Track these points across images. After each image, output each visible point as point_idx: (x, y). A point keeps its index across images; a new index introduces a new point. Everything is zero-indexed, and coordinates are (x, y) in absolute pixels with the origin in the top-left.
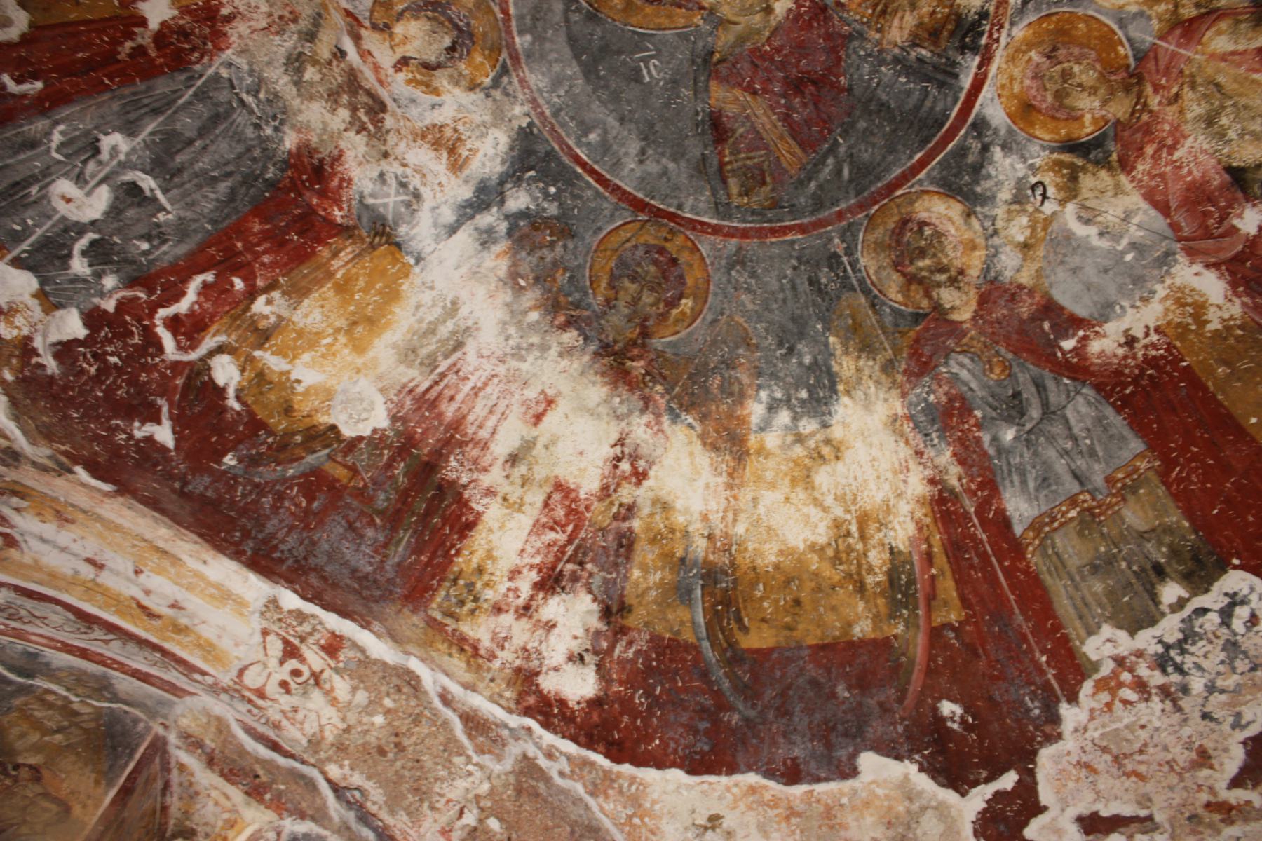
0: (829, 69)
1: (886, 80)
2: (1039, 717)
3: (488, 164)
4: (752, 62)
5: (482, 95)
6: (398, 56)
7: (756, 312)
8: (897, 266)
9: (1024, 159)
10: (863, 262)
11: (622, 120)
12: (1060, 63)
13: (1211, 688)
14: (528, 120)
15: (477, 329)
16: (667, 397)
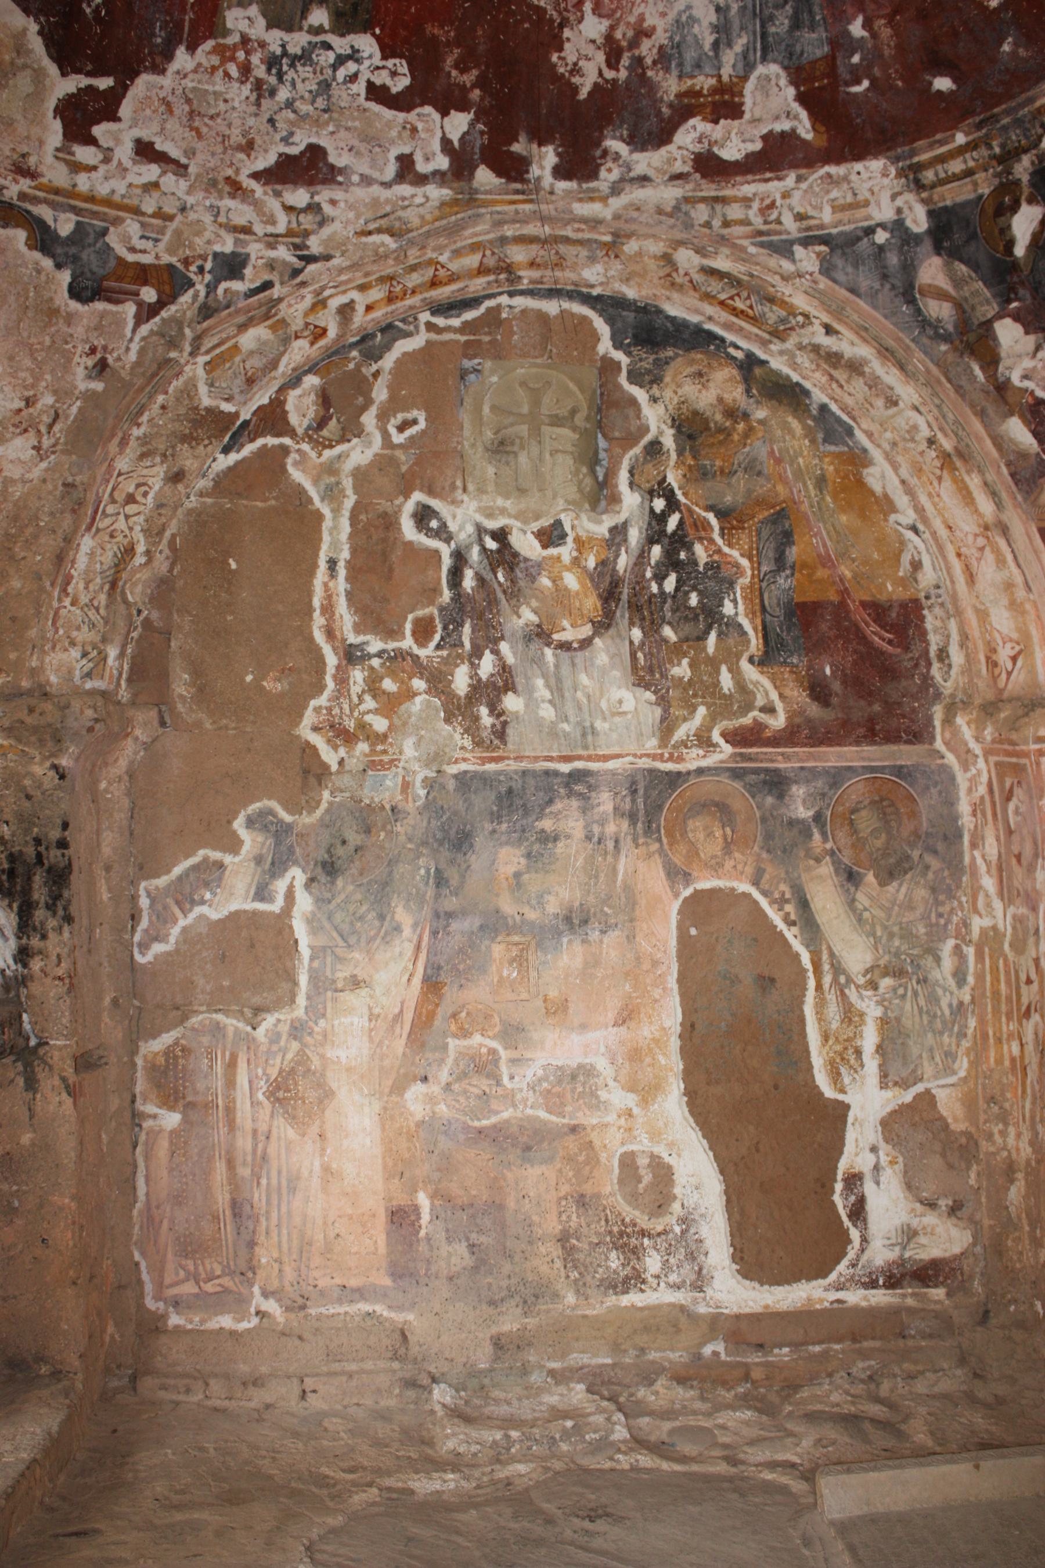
2: (158, 45)
13: (289, 104)
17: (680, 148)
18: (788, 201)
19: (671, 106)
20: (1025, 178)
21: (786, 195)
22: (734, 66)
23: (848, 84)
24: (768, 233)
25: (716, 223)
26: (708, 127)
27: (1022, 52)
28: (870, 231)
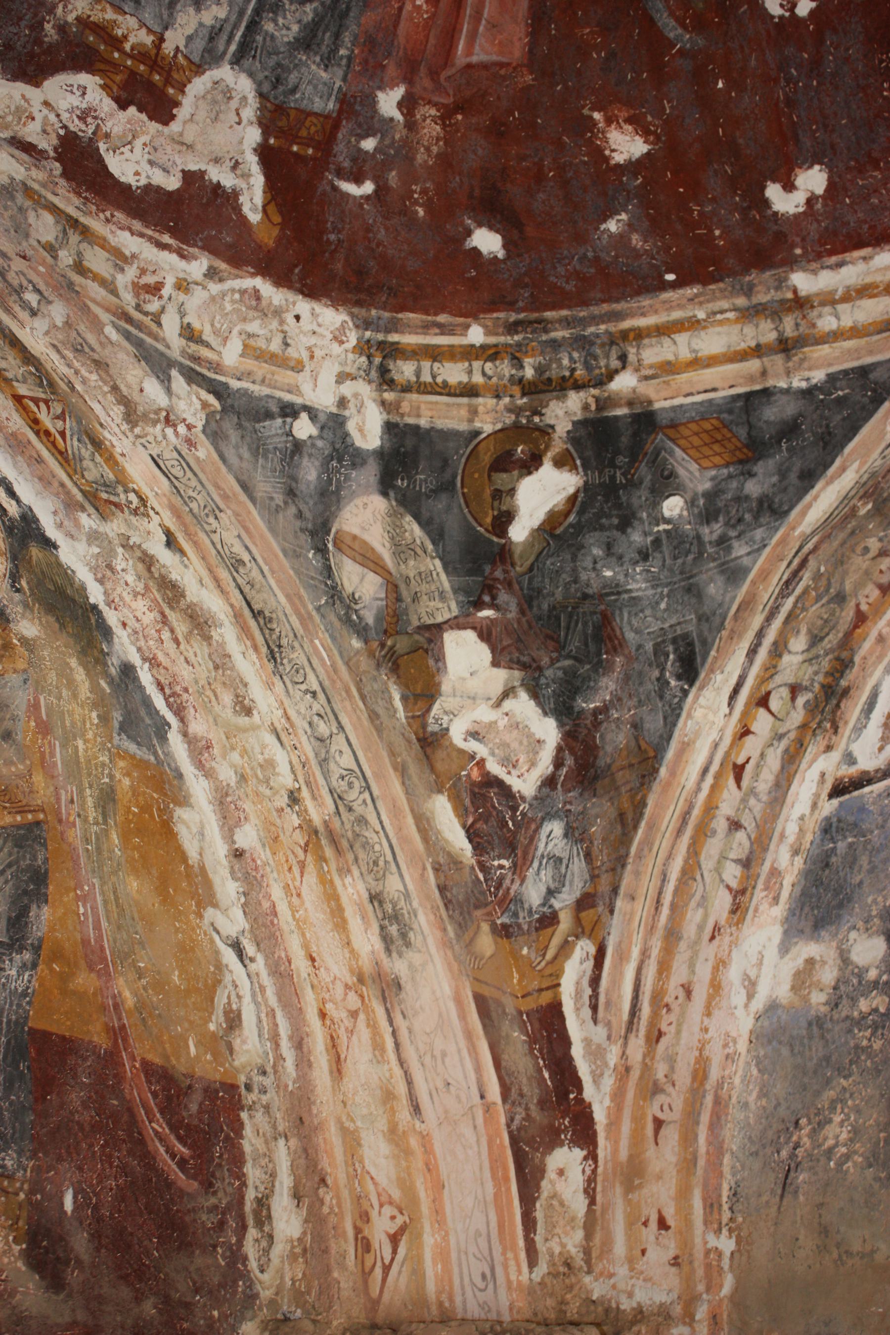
17: (46, 103)
18: (182, 297)
19: (62, 28)
20: (563, 427)
21: (183, 285)
22: (190, 39)
23: (341, 174)
24: (139, 326)
25: (66, 258)
26: (107, 105)
27: (636, 240)
28: (290, 411)
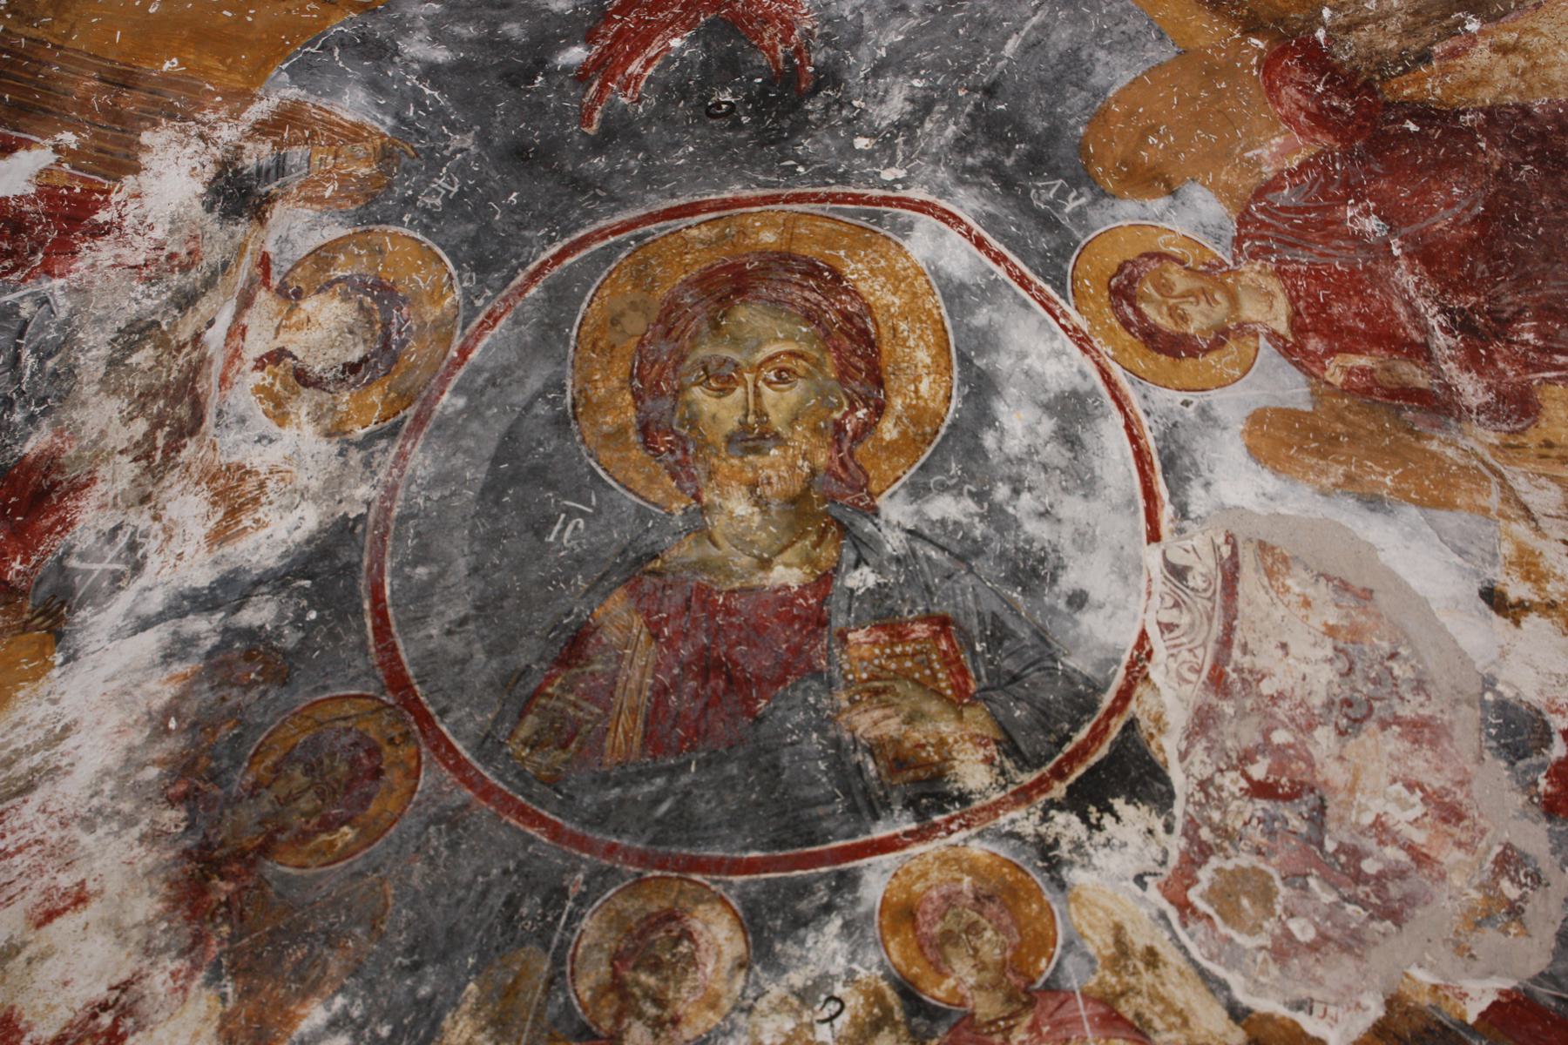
0: (760, 680)
1: (806, 747)
3: (263, 550)
4: (688, 600)
5: (335, 449)
6: (277, 344)
7: (417, 892)
8: (617, 958)
9: (852, 957)
10: (586, 923)
11: (474, 571)
12: (981, 913)
14: (364, 510)
15: (67, 773)
16: (226, 946)
